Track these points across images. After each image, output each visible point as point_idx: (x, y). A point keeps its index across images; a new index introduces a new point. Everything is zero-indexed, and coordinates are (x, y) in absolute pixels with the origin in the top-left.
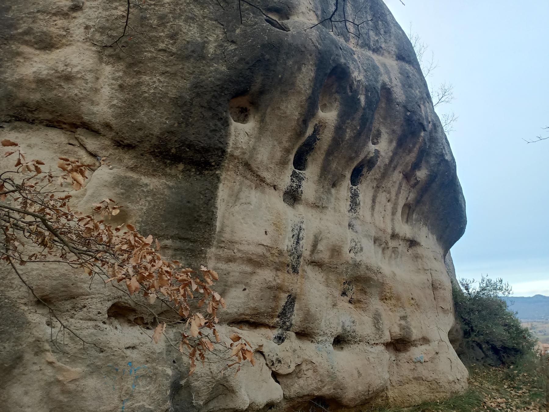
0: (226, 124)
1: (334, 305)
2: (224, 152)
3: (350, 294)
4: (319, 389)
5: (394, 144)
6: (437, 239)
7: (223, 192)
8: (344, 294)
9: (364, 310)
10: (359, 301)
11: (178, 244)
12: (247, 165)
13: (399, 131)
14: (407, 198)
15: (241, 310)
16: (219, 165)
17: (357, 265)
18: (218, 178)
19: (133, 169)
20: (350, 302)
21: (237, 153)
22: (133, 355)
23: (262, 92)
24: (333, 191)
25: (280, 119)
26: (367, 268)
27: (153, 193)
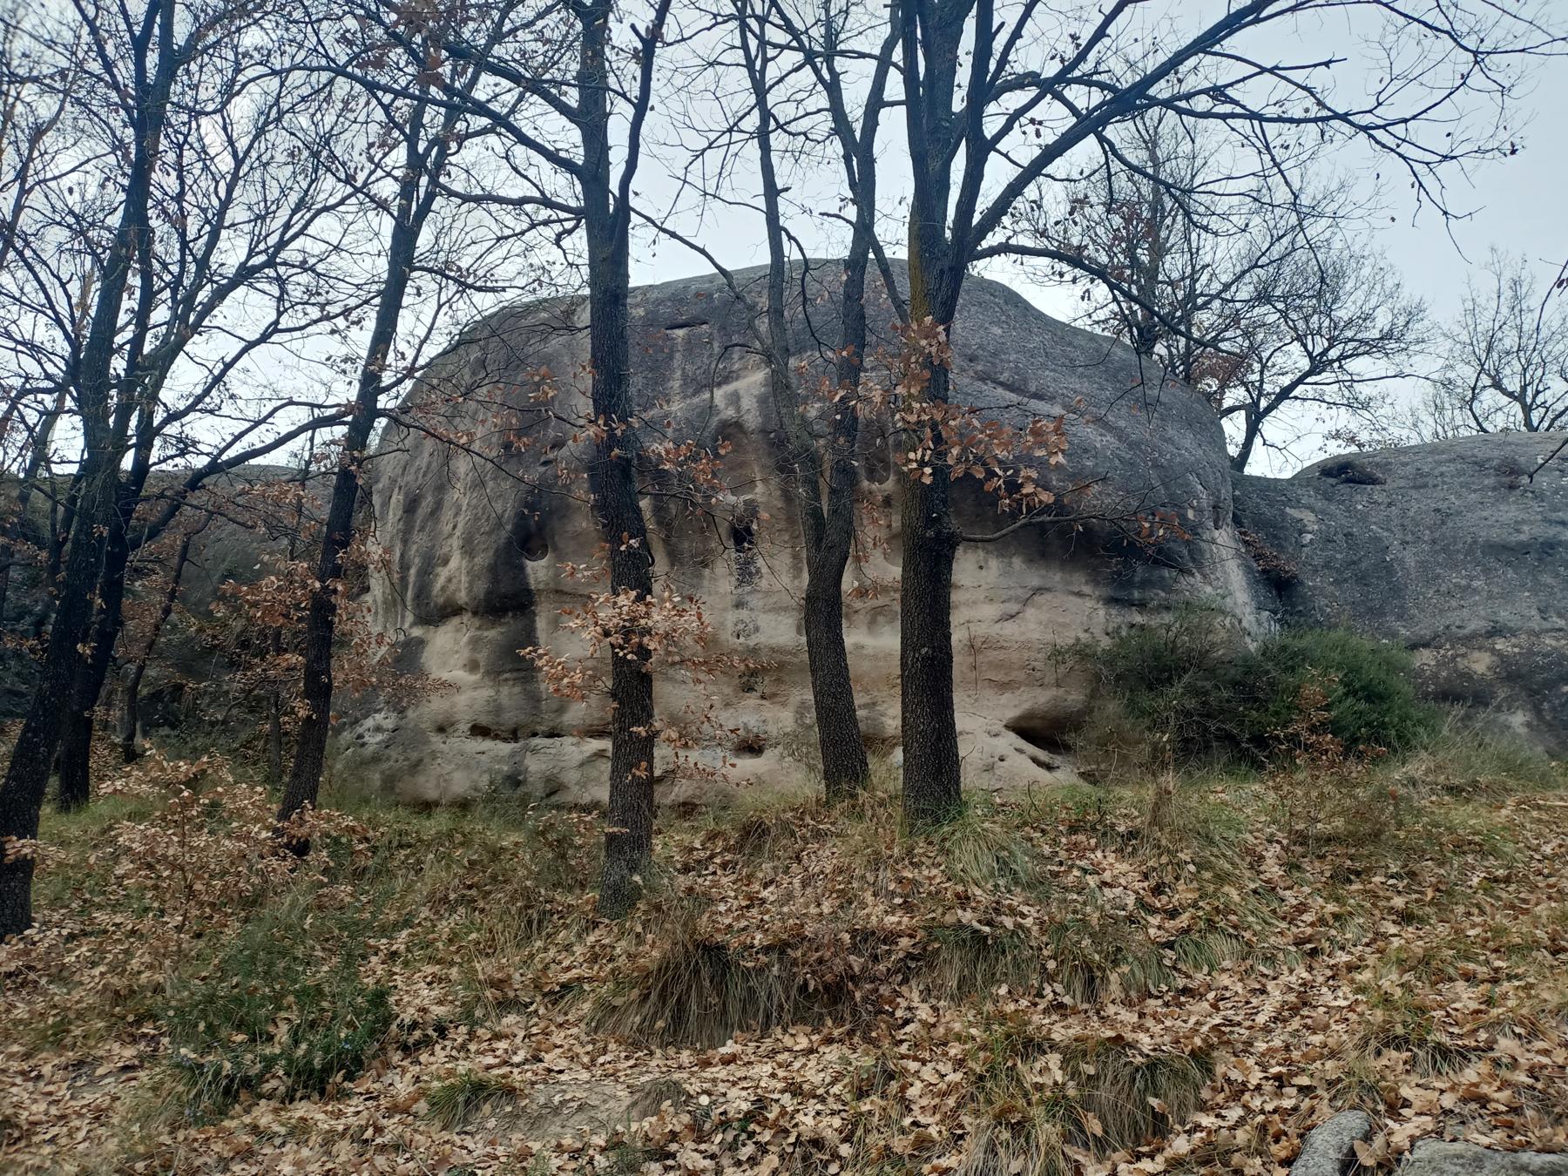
0: (522, 568)
1: (727, 705)
2: (529, 592)
3: (760, 688)
4: (694, 796)
5: (775, 481)
6: (1030, 561)
7: (541, 624)
8: (751, 689)
9: (784, 704)
10: (775, 695)
11: (515, 675)
12: (558, 592)
13: (770, 462)
14: (889, 526)
15: (588, 722)
16: (532, 603)
17: (754, 651)
18: (534, 614)
19: (479, 628)
20: (763, 697)
21: (541, 586)
22: (483, 757)
23: (541, 527)
24: (707, 572)
25: (573, 538)
26: (773, 650)
27: (490, 642)
